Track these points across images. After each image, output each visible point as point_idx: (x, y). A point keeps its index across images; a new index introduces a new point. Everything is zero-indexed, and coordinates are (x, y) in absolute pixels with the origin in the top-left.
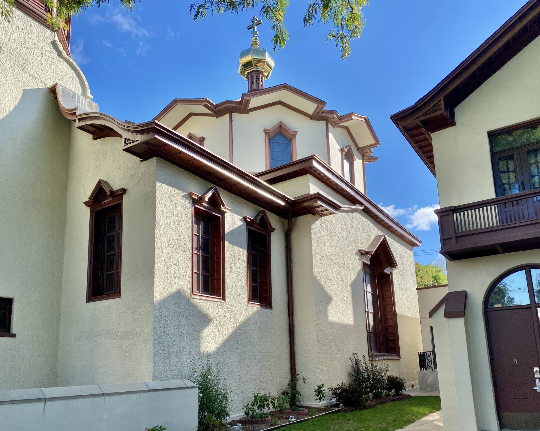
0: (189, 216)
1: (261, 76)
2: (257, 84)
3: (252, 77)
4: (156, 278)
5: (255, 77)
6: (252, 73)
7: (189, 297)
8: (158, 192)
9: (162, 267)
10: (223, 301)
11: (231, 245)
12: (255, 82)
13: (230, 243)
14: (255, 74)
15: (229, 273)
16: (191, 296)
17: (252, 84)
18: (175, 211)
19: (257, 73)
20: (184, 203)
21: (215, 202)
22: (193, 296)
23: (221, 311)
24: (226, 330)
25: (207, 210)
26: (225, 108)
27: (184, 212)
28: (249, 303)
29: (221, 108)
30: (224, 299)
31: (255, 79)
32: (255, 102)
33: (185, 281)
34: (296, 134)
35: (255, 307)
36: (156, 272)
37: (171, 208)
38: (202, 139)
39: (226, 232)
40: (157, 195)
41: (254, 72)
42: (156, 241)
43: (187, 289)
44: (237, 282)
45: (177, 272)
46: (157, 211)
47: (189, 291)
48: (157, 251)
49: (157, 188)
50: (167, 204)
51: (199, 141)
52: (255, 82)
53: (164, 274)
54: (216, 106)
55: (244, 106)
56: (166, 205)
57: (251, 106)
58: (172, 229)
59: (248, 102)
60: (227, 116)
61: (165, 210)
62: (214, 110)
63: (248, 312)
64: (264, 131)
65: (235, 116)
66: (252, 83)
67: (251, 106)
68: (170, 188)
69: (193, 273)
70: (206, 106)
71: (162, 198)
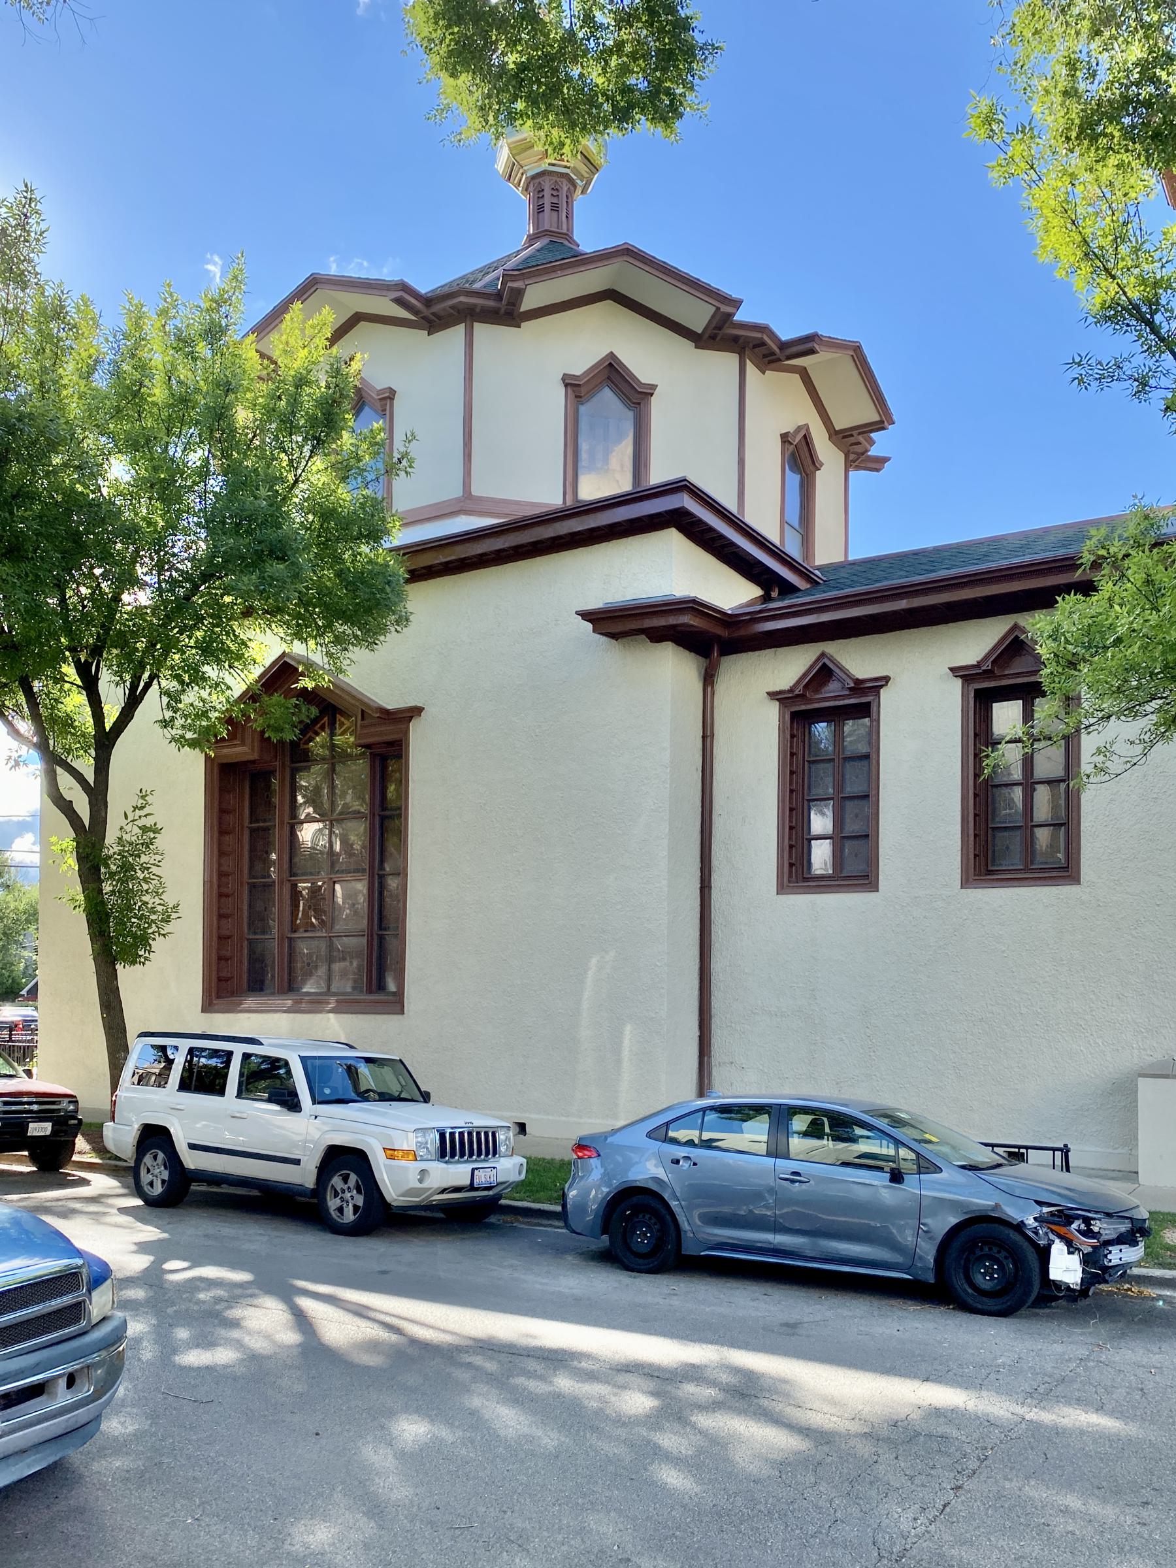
1: (565, 189)
2: (555, 214)
3: (539, 192)
5: (547, 193)
6: (540, 180)
12: (547, 207)
14: (547, 181)
17: (541, 214)
19: (554, 179)
26: (452, 307)
29: (444, 309)
31: (547, 201)
32: (535, 296)
34: (651, 391)
38: (387, 394)
41: (547, 178)
51: (380, 399)
52: (547, 207)
54: (428, 301)
55: (509, 304)
57: (527, 304)
59: (519, 294)
60: (460, 329)
62: (422, 313)
64: (563, 379)
65: (482, 330)
66: (540, 209)
67: (527, 304)
70: (399, 301)
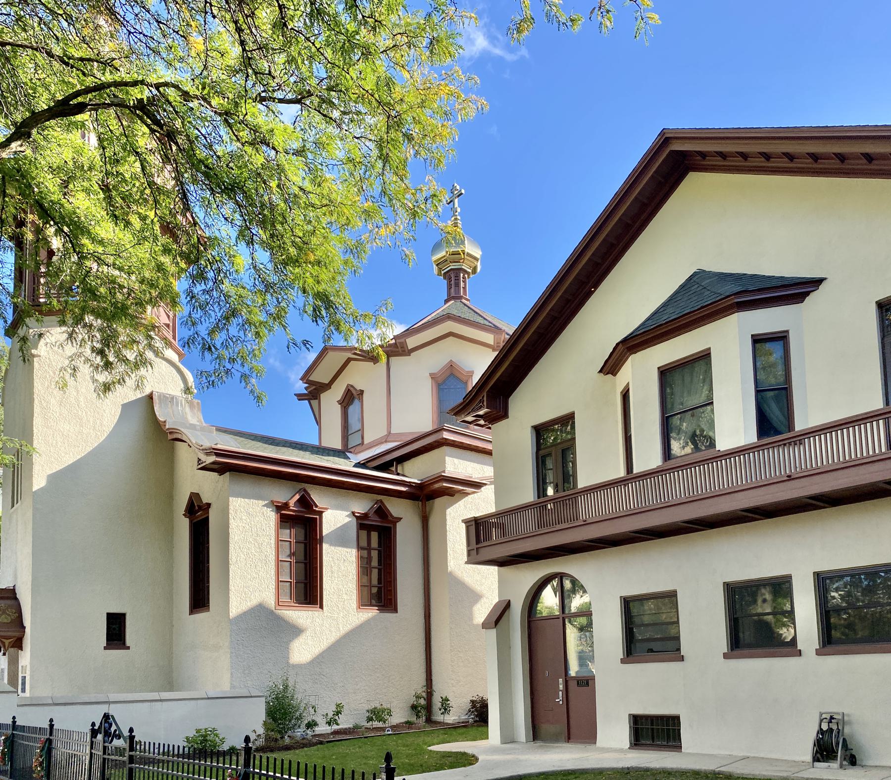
0: (272, 526)
4: (231, 595)
7: (274, 609)
8: (231, 507)
9: (238, 583)
10: (321, 610)
11: (333, 548)
13: (331, 545)
15: (329, 578)
16: (275, 608)
18: (253, 523)
20: (265, 513)
21: (305, 502)
22: (278, 607)
23: (318, 620)
24: (325, 640)
25: (297, 514)
27: (266, 522)
28: (359, 610)
30: (321, 607)
33: (267, 594)
35: (372, 612)
36: (231, 588)
37: (248, 521)
39: (324, 534)
40: (231, 511)
42: (230, 558)
43: (271, 602)
44: (341, 587)
45: (257, 586)
46: (230, 527)
47: (273, 603)
48: (232, 568)
49: (230, 504)
50: (244, 517)
53: (241, 589)
56: (241, 519)
58: (250, 542)
61: (240, 525)
63: (358, 619)
68: (246, 500)
69: (278, 581)
71: (236, 513)
